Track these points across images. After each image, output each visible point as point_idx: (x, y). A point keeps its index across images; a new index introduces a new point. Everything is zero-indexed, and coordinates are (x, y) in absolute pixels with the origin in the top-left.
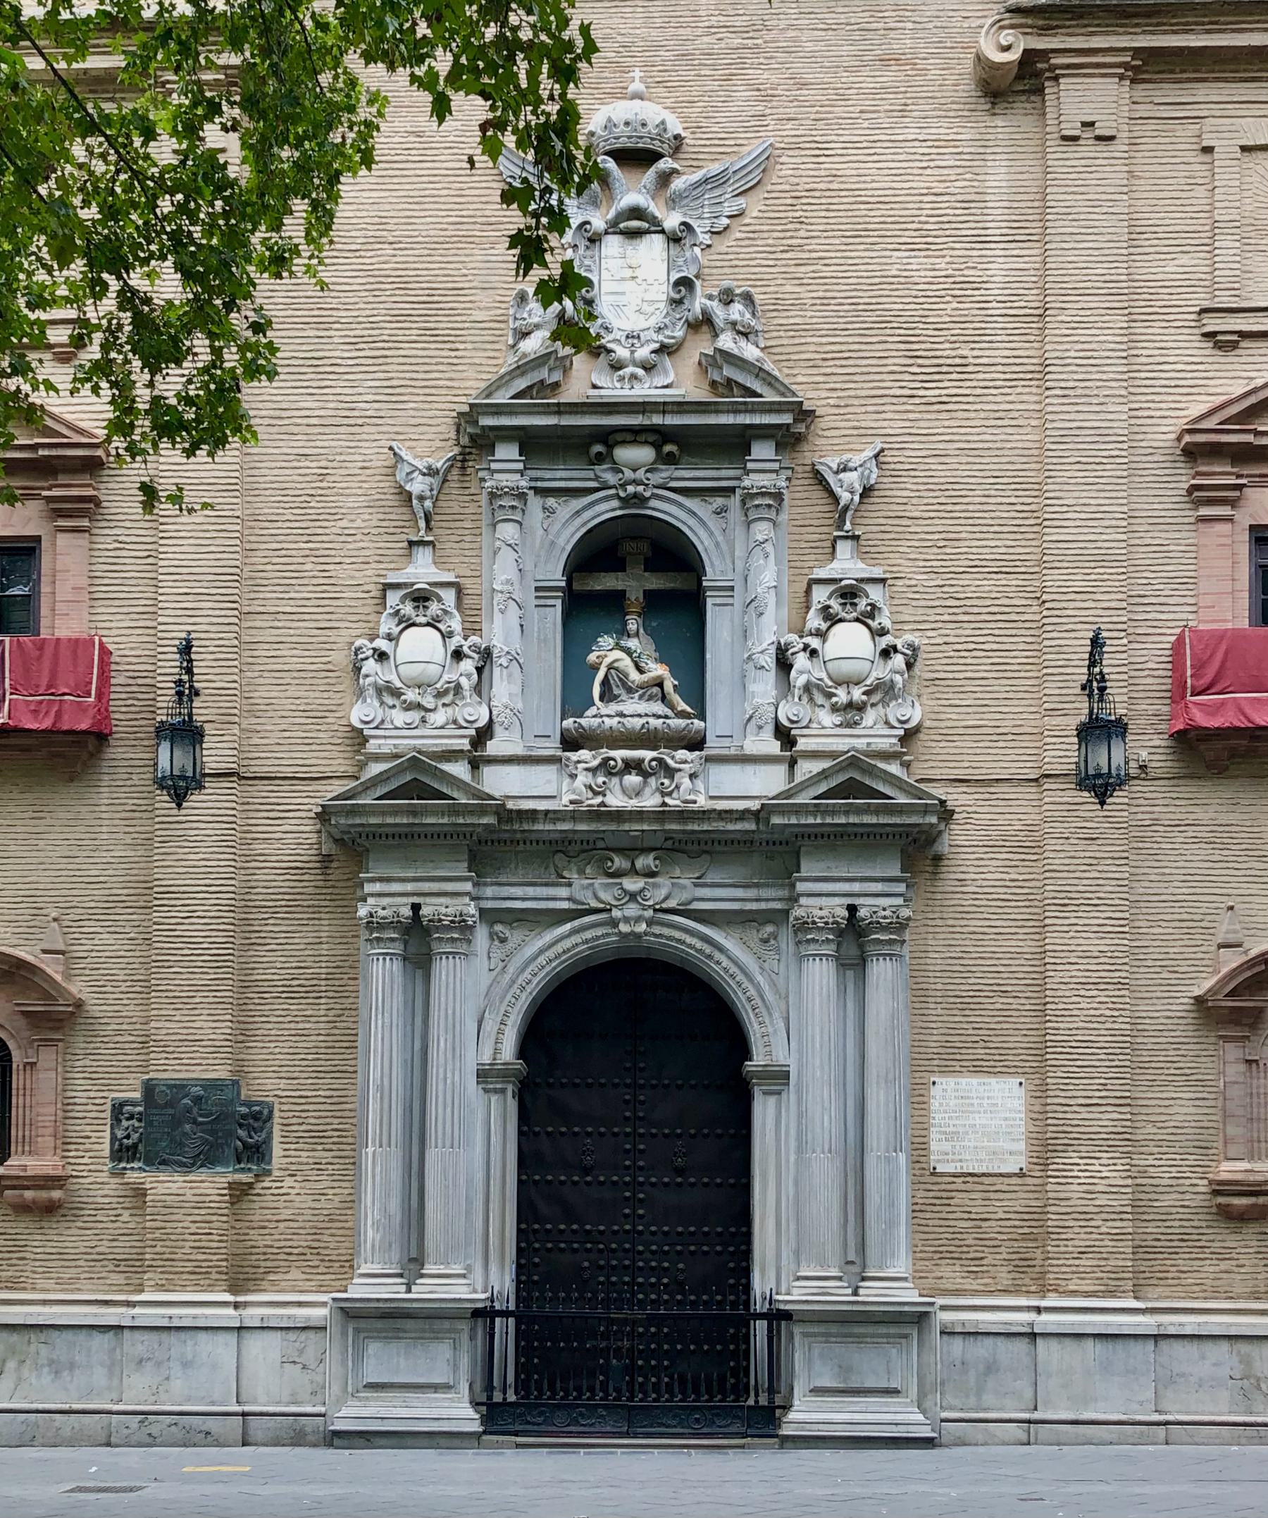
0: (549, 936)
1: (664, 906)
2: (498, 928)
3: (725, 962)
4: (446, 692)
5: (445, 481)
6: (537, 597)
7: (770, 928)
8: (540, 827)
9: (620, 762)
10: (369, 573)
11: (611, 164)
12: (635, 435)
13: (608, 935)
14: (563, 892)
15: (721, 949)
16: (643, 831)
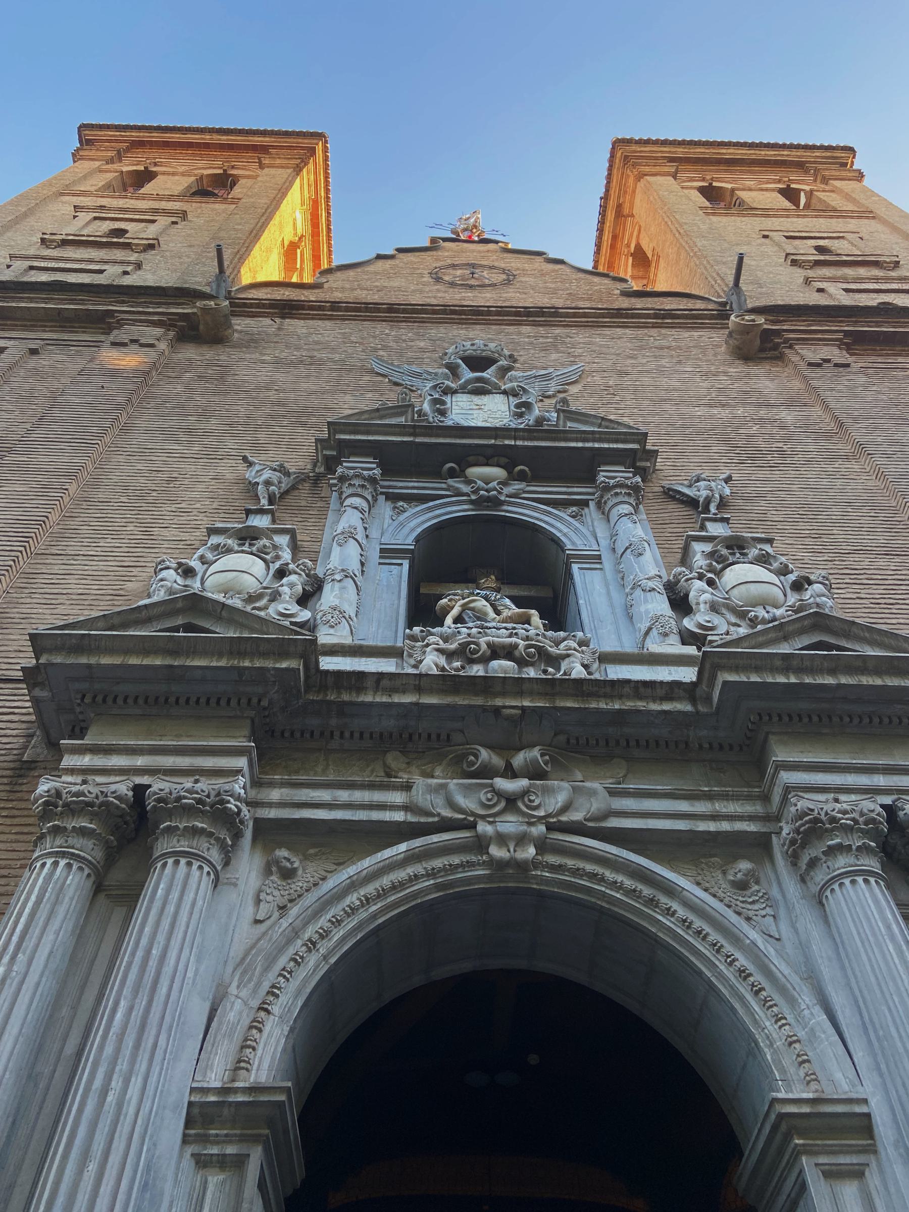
0: (367, 863)
1: (564, 818)
2: (283, 853)
3: (681, 912)
4: (260, 597)
5: (293, 488)
6: (381, 557)
7: (744, 865)
8: (368, 698)
9: (484, 647)
10: (198, 534)
11: (460, 361)
12: (487, 457)
13: (470, 865)
14: (398, 797)
15: (671, 890)
16: (523, 708)
